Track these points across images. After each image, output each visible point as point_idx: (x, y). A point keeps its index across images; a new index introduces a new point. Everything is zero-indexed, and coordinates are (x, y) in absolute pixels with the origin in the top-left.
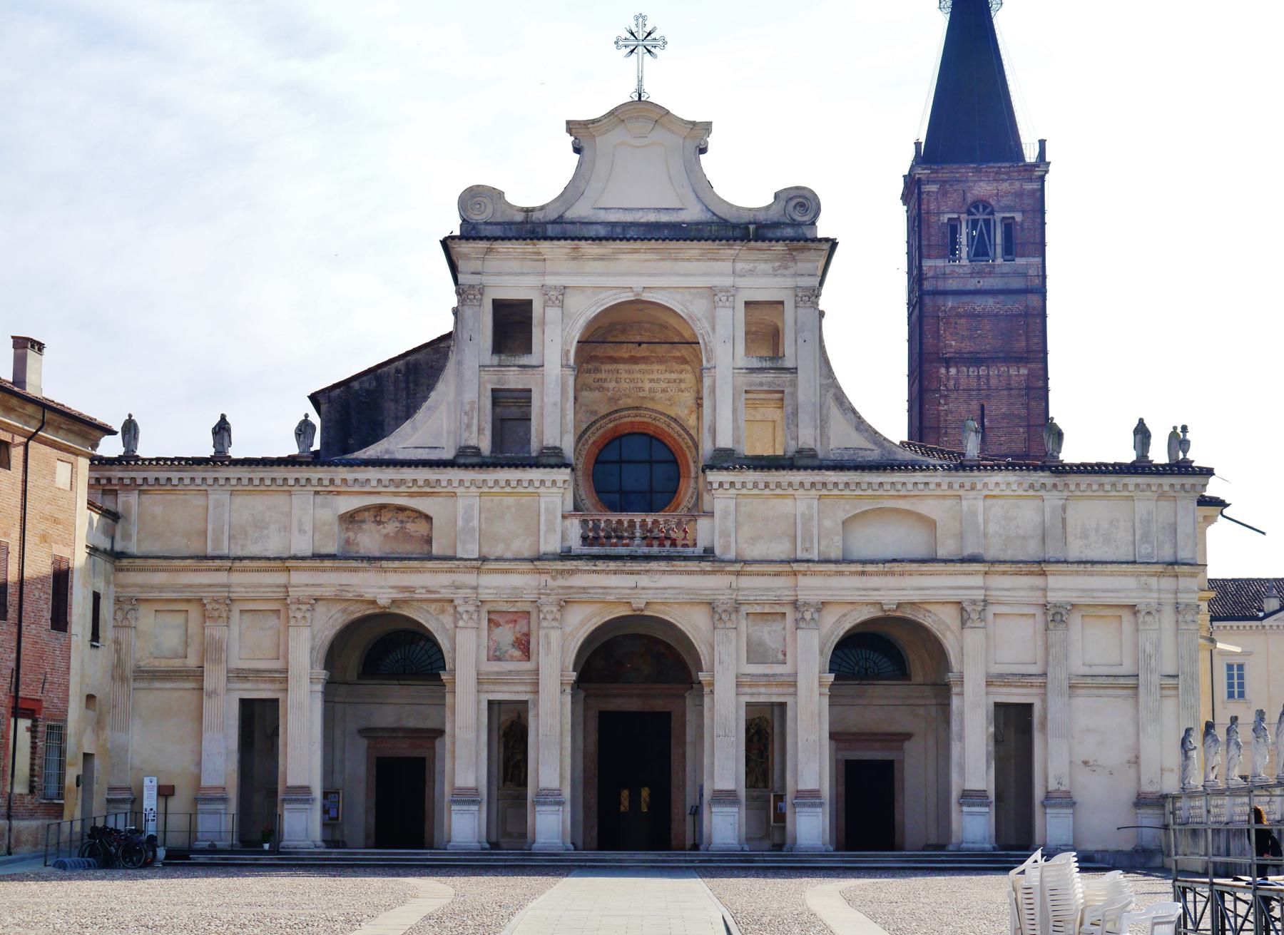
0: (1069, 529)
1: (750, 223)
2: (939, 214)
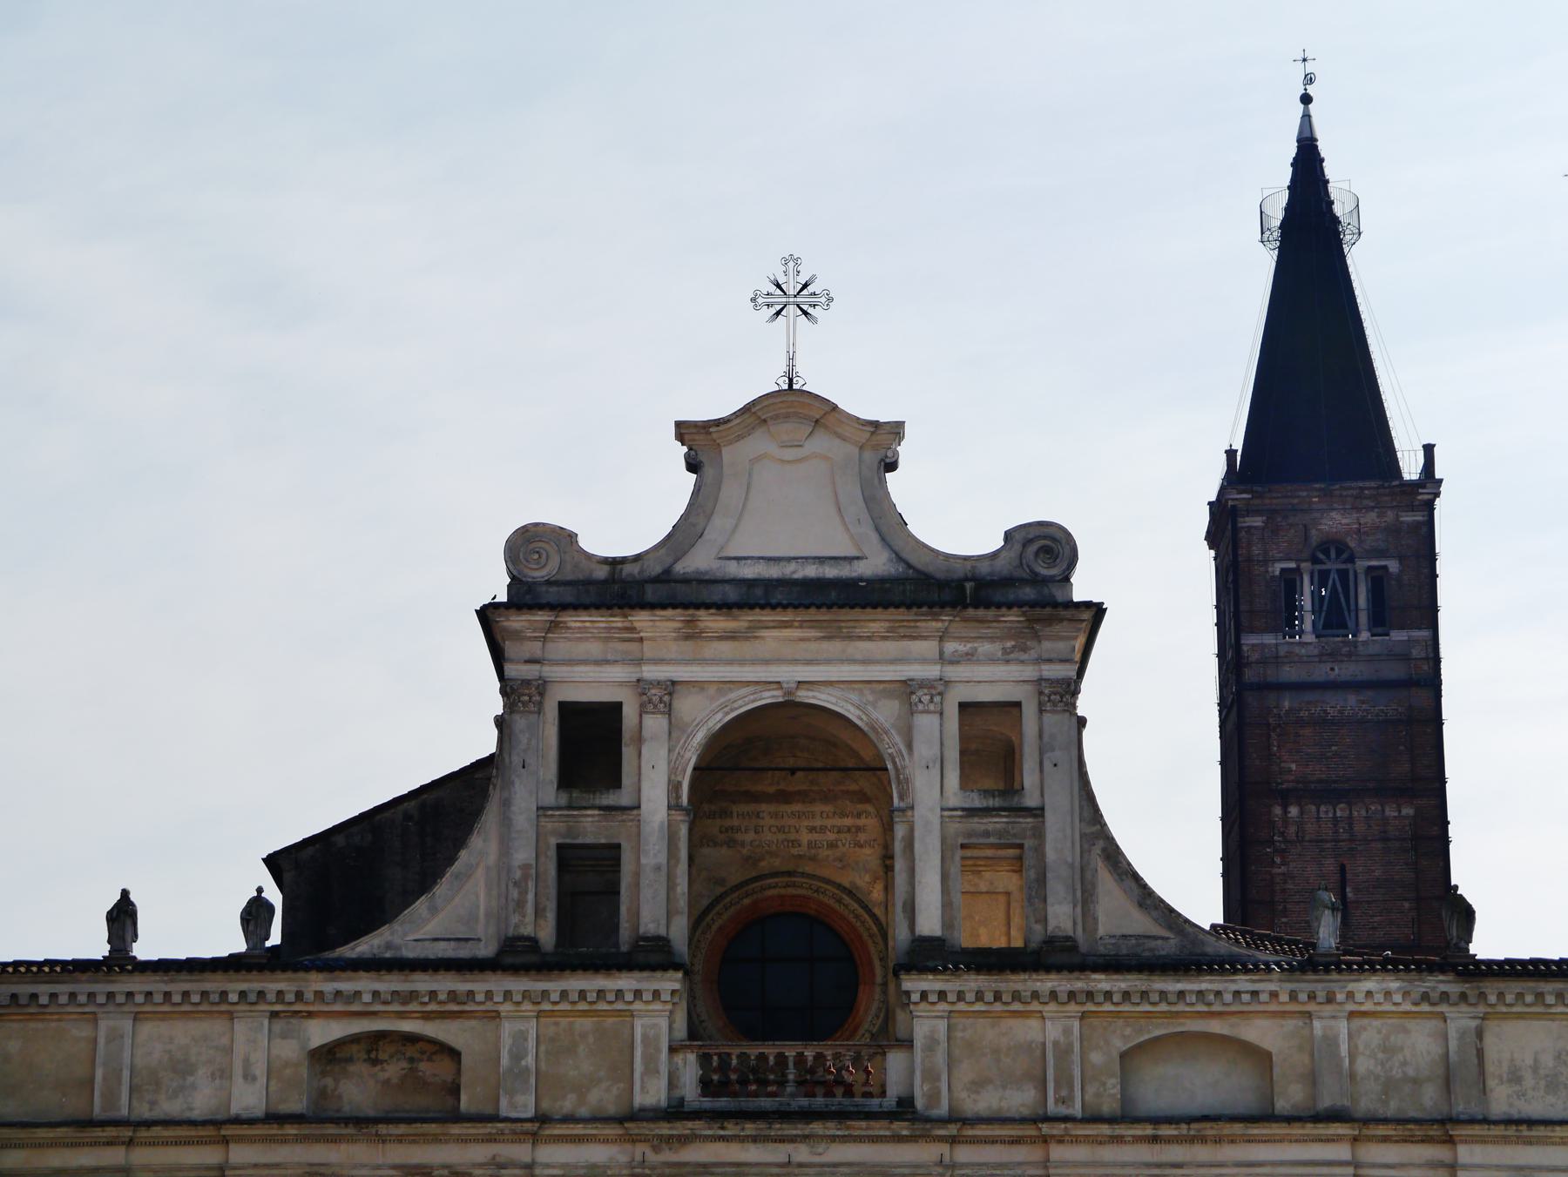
0: (1490, 1068)
1: (967, 579)
2: (1267, 561)
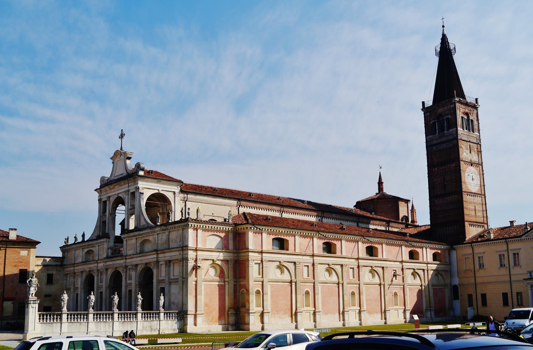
0: (171, 240)
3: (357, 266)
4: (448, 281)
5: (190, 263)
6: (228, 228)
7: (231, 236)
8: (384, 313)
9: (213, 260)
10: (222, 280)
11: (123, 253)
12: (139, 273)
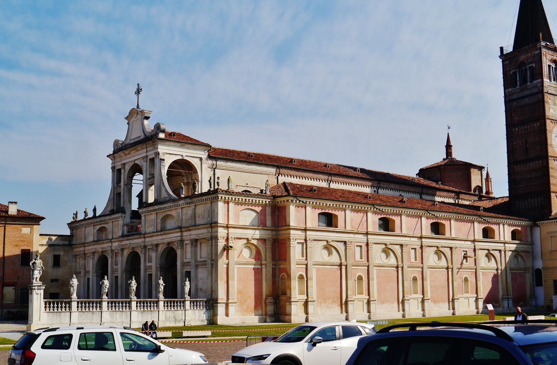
0: (197, 215)
3: (420, 246)
4: (529, 264)
5: (220, 242)
6: (266, 201)
7: (268, 210)
8: (452, 301)
9: (248, 239)
10: (258, 262)
11: (141, 231)
12: (161, 254)
